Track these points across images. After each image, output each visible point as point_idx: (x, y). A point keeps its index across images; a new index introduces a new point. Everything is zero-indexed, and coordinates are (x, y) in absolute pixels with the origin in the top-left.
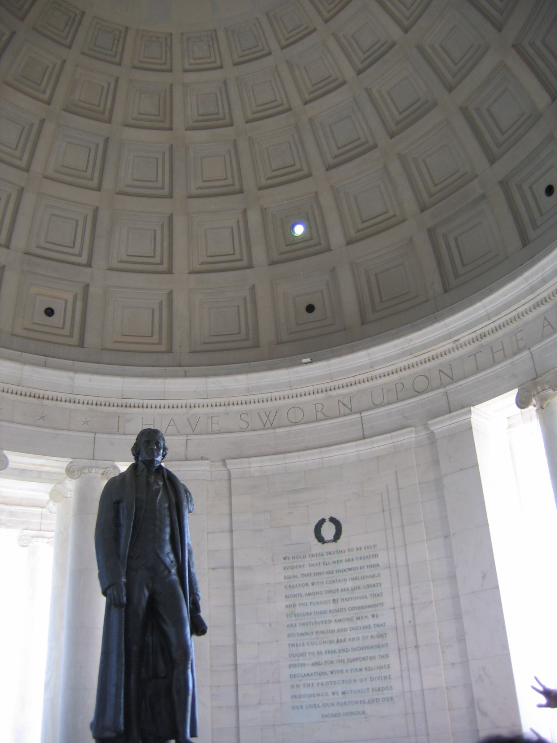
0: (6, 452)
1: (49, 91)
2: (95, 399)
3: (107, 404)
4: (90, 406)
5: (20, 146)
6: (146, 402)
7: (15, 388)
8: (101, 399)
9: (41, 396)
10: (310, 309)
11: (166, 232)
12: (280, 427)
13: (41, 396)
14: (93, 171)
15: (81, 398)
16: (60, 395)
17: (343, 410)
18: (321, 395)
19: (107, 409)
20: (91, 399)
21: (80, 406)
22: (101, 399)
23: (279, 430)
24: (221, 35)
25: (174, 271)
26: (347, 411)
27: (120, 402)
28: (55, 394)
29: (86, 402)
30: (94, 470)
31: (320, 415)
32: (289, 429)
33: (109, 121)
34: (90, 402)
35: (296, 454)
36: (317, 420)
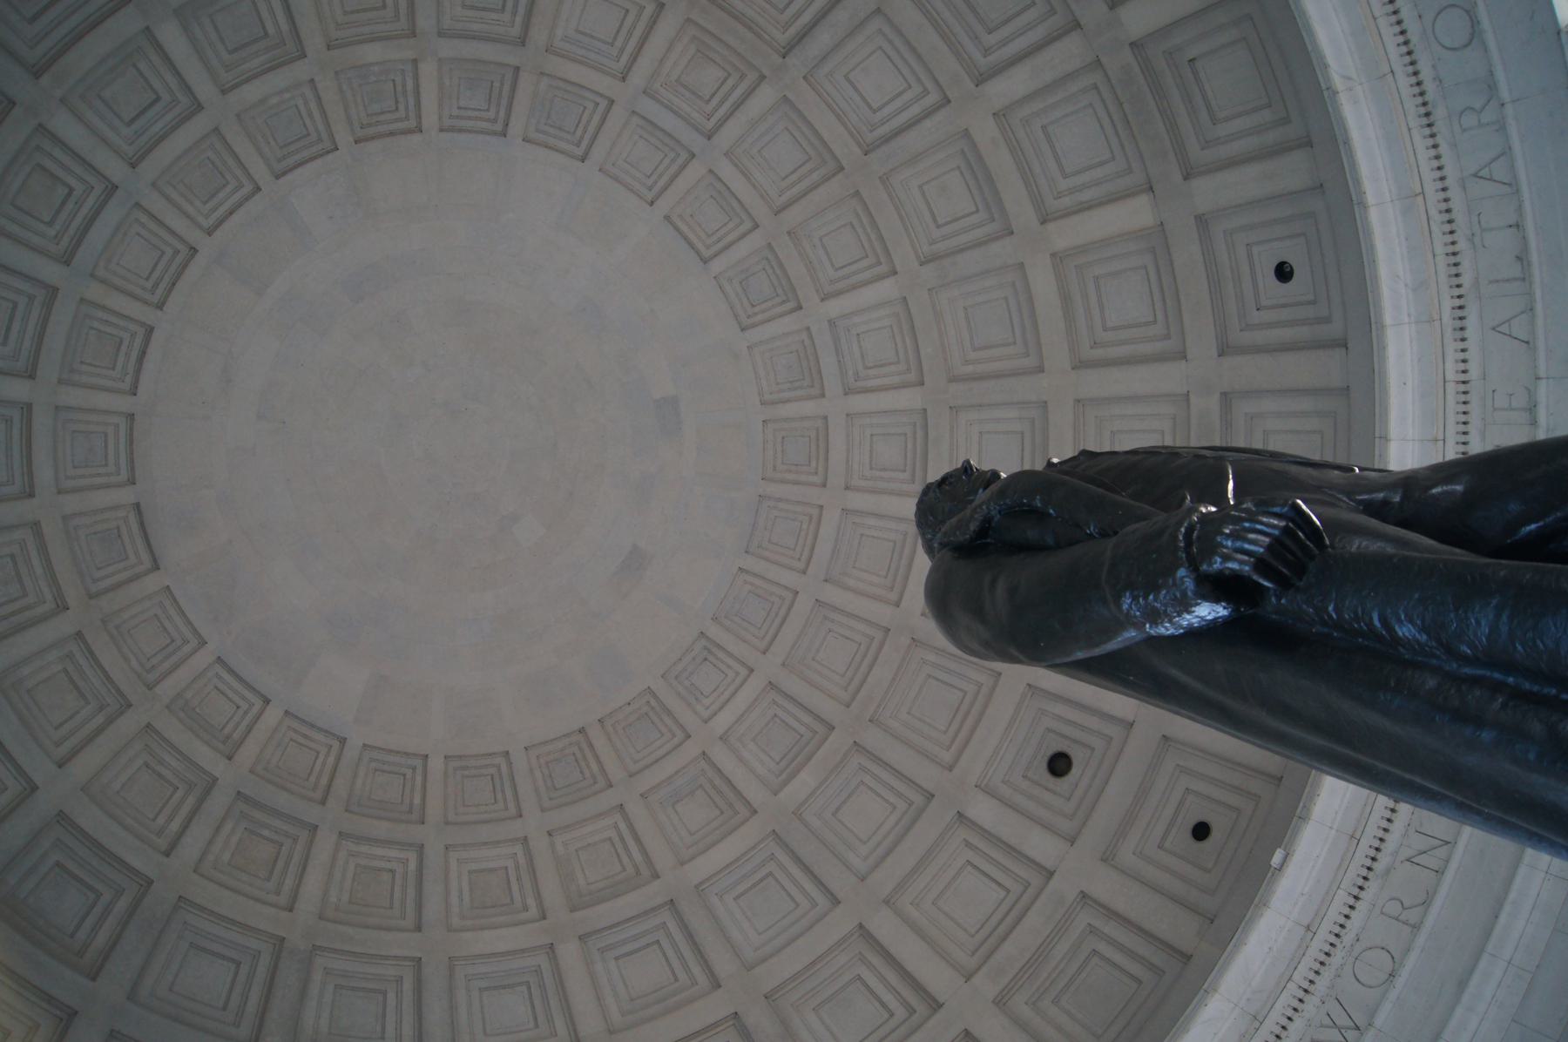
1: (531, 902)
5: (541, 1018)
10: (1201, 831)
11: (876, 961)
12: (1373, 1013)
14: (687, 970)
17: (1430, 861)
18: (1372, 887)
23: (1379, 1021)
24: (714, 631)
25: (941, 1000)
26: (1442, 852)
31: (1413, 916)
32: (1393, 995)
33: (656, 876)
35: (1459, 1011)
36: (1416, 927)
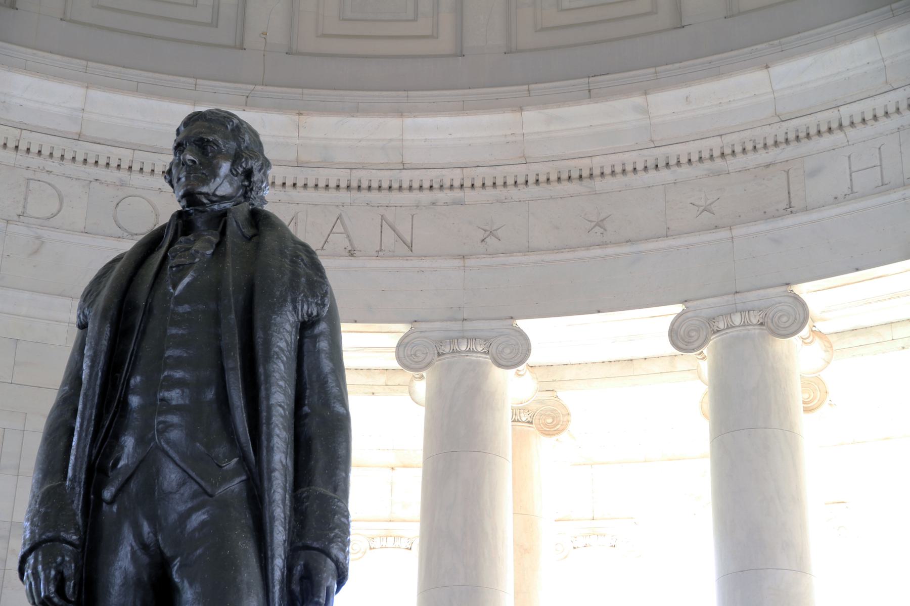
0: (522, 324)
2: (715, 144)
3: (749, 147)
4: (707, 165)
6: (845, 112)
7: (520, 171)
8: (728, 139)
9: (585, 173)
13: (585, 173)
15: (681, 150)
16: (629, 158)
19: (751, 159)
20: (705, 146)
21: (685, 170)
22: (728, 139)
27: (779, 131)
28: (617, 159)
29: (695, 158)
30: (737, 319)
34: (706, 155)
